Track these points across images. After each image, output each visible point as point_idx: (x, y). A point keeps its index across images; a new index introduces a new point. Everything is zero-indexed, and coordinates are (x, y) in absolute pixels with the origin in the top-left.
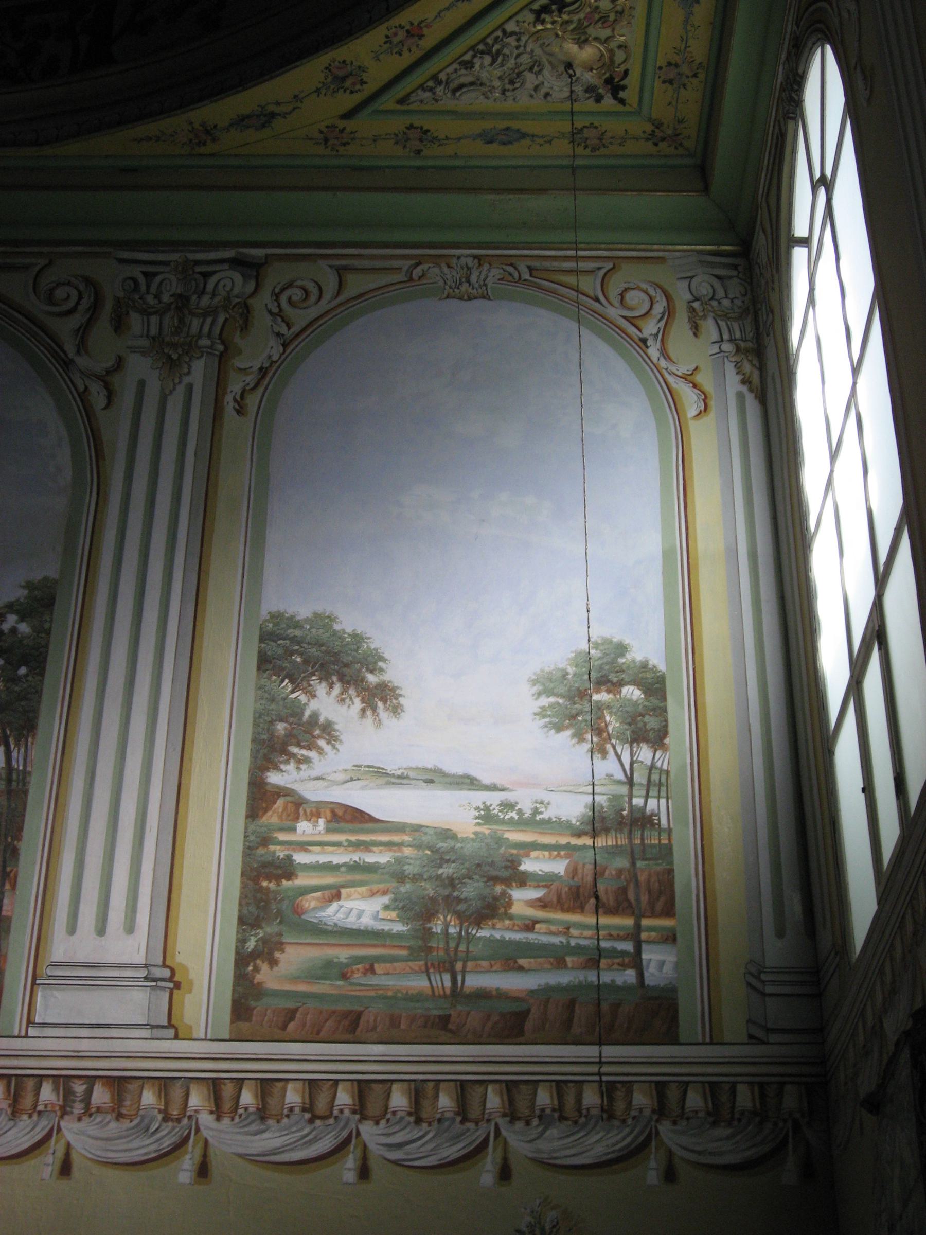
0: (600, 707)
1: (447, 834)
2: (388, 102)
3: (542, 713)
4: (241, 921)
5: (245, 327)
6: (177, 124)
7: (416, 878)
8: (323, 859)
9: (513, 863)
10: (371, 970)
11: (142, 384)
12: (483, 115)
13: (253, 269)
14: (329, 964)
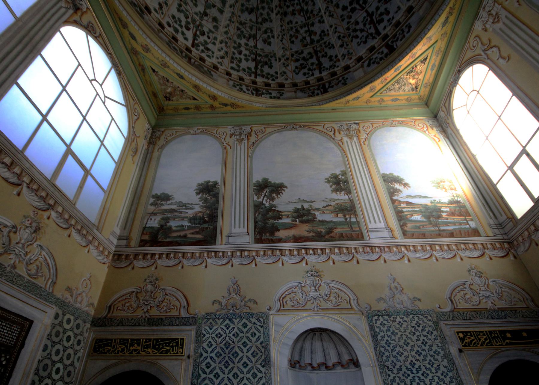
2: (378, 94)
6: (343, 100)
12: (393, 96)
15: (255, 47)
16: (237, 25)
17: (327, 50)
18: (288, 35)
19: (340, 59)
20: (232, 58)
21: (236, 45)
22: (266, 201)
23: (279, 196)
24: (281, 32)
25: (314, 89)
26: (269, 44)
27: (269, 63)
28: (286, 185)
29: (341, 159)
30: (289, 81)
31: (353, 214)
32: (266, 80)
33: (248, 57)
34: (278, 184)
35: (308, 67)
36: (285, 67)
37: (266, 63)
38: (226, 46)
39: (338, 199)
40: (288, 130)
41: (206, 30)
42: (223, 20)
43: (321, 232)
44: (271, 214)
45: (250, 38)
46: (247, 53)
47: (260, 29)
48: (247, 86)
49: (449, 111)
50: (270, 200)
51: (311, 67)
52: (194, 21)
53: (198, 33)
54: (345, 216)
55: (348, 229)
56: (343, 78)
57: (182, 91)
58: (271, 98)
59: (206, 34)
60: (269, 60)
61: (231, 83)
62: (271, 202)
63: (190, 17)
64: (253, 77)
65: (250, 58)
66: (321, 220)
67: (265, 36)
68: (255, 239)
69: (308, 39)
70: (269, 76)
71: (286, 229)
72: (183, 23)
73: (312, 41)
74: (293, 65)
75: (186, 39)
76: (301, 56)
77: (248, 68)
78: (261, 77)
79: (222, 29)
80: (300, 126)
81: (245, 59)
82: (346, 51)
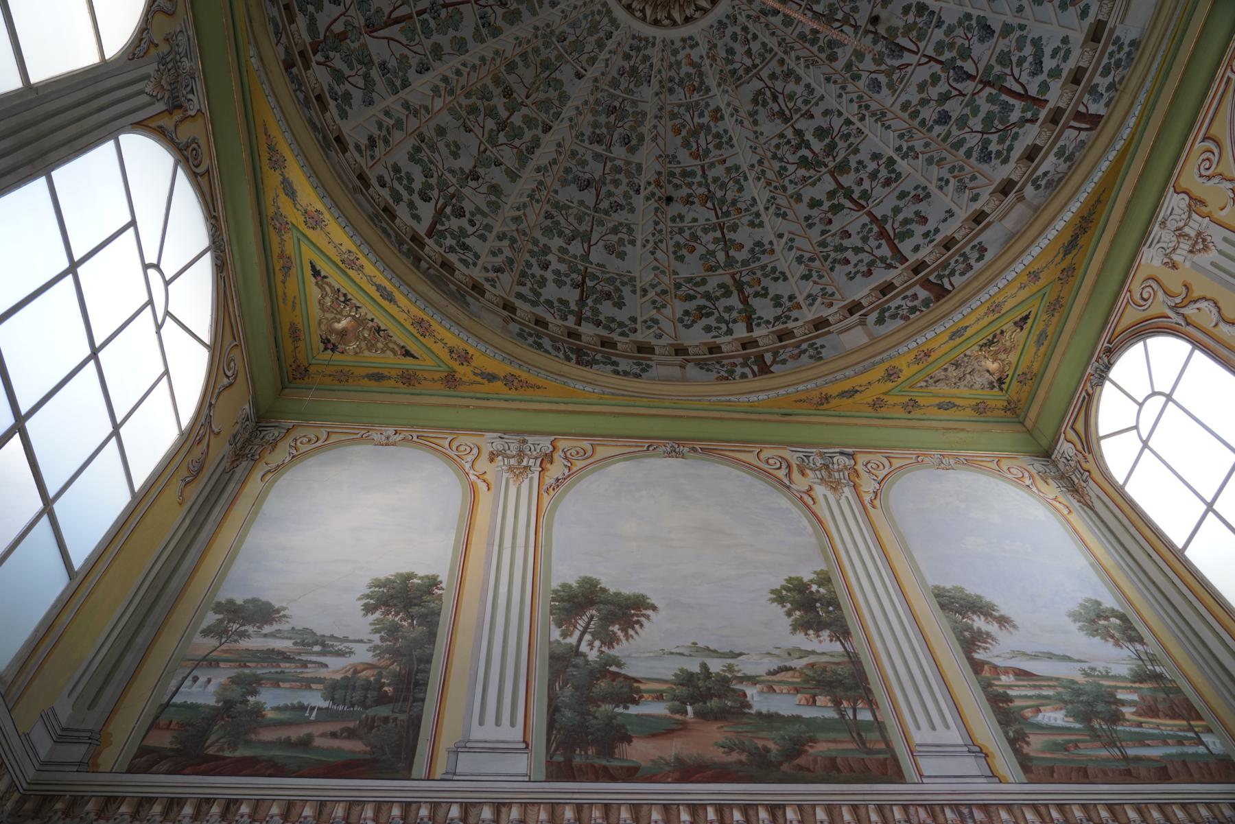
0: (1105, 627)
1: (1073, 682)
3: (1081, 629)
4: (1000, 723)
5: (858, 476)
7: (1072, 702)
8: (1023, 693)
9: (1113, 695)
10: (1077, 747)
11: (825, 496)
13: (851, 456)
14: (1055, 743)
15: (586, 257)
16: (547, 207)
17: (766, 282)
18: (671, 243)
20: (523, 274)
21: (536, 249)
22: (591, 644)
23: (631, 632)
24: (654, 235)
25: (735, 365)
26: (622, 256)
28: (653, 600)
29: (813, 540)
30: (665, 341)
31: (862, 697)
32: (605, 333)
33: (563, 278)
34: (628, 598)
35: (717, 314)
37: (608, 296)
38: (511, 247)
39: (813, 652)
40: (658, 456)
41: (468, 206)
42: (515, 194)
43: (767, 750)
44: (603, 684)
46: (563, 268)
47: (601, 223)
48: (554, 339)
49: (1088, 443)
50: (603, 643)
51: (726, 316)
52: (442, 186)
53: (448, 210)
54: (837, 704)
55: (852, 746)
56: (811, 345)
57: (379, 330)
58: (616, 372)
59: (467, 214)
60: (617, 289)
61: (514, 328)
62: (605, 649)
63: (435, 175)
64: (571, 322)
66: (764, 711)
67: (613, 238)
68: (549, 763)
69: (721, 256)
70: (612, 325)
71: (653, 736)
72: (417, 185)
74: (679, 307)
75: (417, 218)
76: (701, 289)
77: (560, 301)
78: (591, 325)
79: (507, 211)
80: (694, 450)
81: (556, 281)
82: (818, 287)
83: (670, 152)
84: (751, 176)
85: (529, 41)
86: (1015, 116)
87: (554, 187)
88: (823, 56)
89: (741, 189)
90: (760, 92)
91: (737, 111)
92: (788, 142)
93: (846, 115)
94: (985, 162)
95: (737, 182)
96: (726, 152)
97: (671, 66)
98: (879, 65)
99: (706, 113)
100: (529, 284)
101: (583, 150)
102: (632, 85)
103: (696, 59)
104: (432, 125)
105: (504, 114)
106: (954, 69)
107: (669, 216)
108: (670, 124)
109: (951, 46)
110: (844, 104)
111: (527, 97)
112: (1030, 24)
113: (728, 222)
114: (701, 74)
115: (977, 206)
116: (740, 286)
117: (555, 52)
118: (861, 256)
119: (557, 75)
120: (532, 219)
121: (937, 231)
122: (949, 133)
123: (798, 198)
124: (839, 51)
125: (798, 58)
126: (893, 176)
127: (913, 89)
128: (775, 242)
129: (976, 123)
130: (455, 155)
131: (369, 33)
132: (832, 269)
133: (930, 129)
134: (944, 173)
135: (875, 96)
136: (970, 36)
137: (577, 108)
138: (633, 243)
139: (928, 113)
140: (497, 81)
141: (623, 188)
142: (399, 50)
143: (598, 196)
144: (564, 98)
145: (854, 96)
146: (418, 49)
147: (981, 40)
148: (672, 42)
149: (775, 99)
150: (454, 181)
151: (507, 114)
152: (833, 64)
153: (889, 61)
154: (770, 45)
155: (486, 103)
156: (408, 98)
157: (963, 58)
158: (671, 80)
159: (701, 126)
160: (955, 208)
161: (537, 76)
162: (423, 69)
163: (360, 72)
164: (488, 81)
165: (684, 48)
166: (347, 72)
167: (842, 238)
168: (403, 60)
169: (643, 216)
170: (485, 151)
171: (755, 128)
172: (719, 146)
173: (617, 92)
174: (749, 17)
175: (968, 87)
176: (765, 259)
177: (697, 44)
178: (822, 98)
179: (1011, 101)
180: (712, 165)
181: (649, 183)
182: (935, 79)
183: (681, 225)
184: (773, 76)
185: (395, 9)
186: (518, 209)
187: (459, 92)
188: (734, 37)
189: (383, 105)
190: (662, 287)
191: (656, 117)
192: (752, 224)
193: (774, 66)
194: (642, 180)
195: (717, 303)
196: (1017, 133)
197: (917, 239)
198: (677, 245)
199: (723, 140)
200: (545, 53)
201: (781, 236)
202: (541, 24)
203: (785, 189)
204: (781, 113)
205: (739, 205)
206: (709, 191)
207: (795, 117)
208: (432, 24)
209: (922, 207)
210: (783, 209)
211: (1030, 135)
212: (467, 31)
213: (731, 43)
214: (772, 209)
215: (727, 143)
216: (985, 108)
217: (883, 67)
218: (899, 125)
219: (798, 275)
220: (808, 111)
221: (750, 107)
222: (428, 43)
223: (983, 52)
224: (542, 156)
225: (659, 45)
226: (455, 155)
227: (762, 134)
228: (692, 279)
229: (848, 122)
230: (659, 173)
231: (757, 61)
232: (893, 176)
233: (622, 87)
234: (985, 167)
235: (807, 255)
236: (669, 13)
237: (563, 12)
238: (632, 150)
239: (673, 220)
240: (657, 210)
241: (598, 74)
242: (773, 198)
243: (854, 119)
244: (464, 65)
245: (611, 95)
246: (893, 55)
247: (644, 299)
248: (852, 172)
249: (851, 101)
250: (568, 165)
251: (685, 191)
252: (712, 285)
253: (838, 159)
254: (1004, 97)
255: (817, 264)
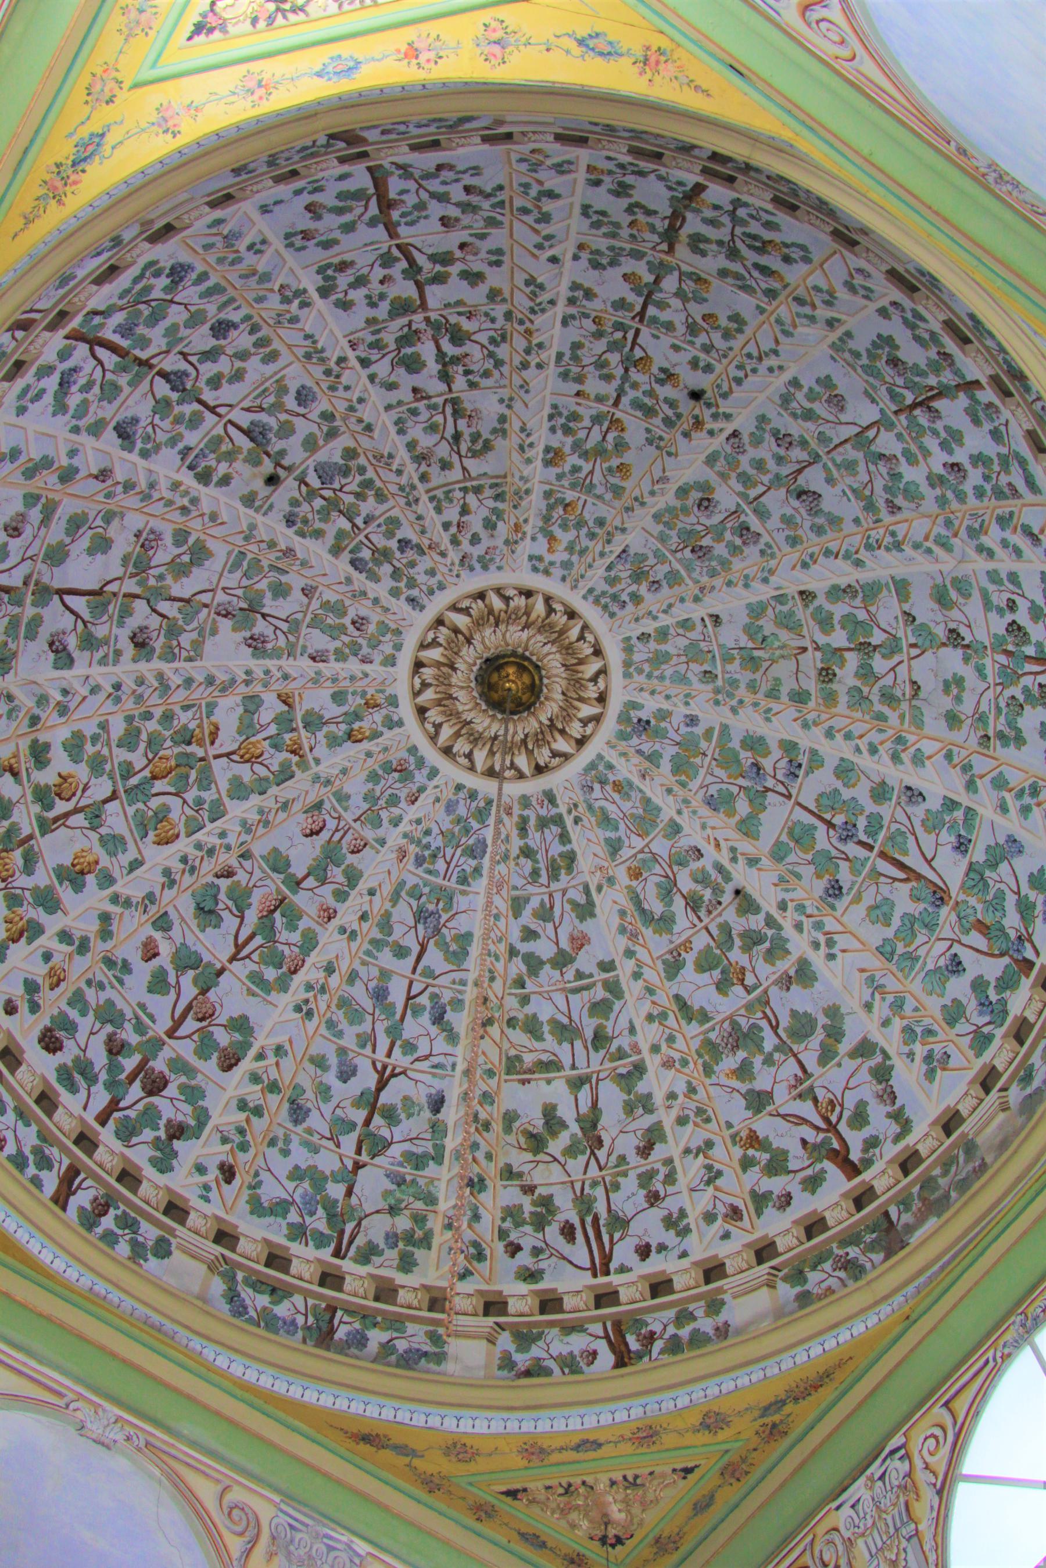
15: (882, 423)
18: (737, 343)
19: (583, 168)
20: (999, 493)
21: (949, 495)
24: (754, 371)
27: (884, 353)
33: (943, 435)
35: (738, 231)
36: (831, 293)
37: (894, 362)
38: (983, 530)
41: (999, 625)
45: (882, 456)
46: (932, 444)
47: (822, 438)
53: (1030, 651)
59: (1009, 617)
63: (1007, 693)
65: (939, 426)
67: (820, 409)
69: (670, 283)
70: (926, 336)
73: (660, 271)
74: (794, 274)
76: (736, 267)
77: (976, 422)
79: (947, 564)
82: (542, 175)
83: (651, 450)
84: (549, 355)
85: (755, 705)
86: (119, 318)
87: (854, 529)
88: (362, 461)
89: (576, 346)
90: (475, 454)
91: (521, 448)
92: (467, 373)
93: (364, 373)
94: (182, 266)
95: (575, 358)
96: (569, 404)
97: (583, 552)
98: (287, 422)
99: (567, 468)
100: (1004, 479)
101: (775, 534)
102: (652, 561)
103: (542, 541)
104: (958, 736)
105: (852, 660)
106: (184, 390)
107: (712, 377)
108: (627, 484)
109: (178, 420)
110: (360, 387)
111: (804, 650)
112: (64, 434)
113: (625, 317)
114: (547, 519)
115: (218, 214)
116: (670, 236)
117: (729, 667)
118: (442, 189)
119: (744, 641)
120: (919, 528)
121: (298, 193)
122: (220, 309)
123: (494, 295)
124: (337, 459)
125: (399, 472)
126: (330, 272)
127: (251, 377)
128: (569, 256)
129: (176, 315)
130: (959, 681)
131: (946, 891)
132: (500, 188)
133: (248, 318)
134: (250, 259)
135: (310, 383)
136: (150, 429)
137: (746, 586)
138: (795, 383)
139: (241, 339)
140: (830, 699)
141: (752, 453)
142: (927, 841)
143: (799, 471)
144: (756, 611)
145: (341, 393)
146: (901, 817)
147: (135, 421)
148: (564, 579)
149: (457, 437)
150: (988, 661)
151: (847, 655)
152: (352, 444)
153: (272, 422)
154: (431, 506)
155: (865, 690)
156: (962, 790)
157: (167, 403)
158: (592, 536)
159: (585, 455)
160: (255, 215)
161: (773, 661)
162: (913, 795)
163: (994, 875)
164: (842, 707)
165: (551, 564)
166: (1011, 900)
167: (457, 220)
168: (933, 823)
169: (751, 403)
170: (913, 646)
171: (507, 412)
172: (574, 417)
173: (677, 566)
174: (443, 554)
175: (172, 363)
176: (602, 244)
177: (531, 558)
178: (388, 408)
179: (116, 339)
180: (600, 399)
181: (711, 433)
182: (215, 383)
183: (702, 356)
184: (445, 465)
185: (895, 879)
186: (929, 551)
187: (891, 732)
188: (475, 540)
189: (998, 819)
190: (796, 308)
191: (643, 504)
192: (589, 294)
193: (438, 477)
194: (718, 443)
195: (727, 238)
196: (121, 298)
197: (334, 189)
198: (727, 335)
199: (564, 421)
200: (744, 677)
201: (554, 260)
202: (726, 710)
203: (508, 316)
204: (457, 413)
205: (593, 328)
206: (626, 370)
207: (440, 401)
208: (862, 823)
209: (305, 222)
210: (528, 290)
211: (101, 297)
212: (822, 780)
213: (483, 534)
214: (544, 297)
215: (560, 414)
216: (157, 336)
217: (283, 417)
218: (290, 335)
219: (560, 203)
220: (417, 400)
221: (499, 443)
222: (886, 810)
223: (137, 403)
224: (844, 574)
225: (584, 587)
226: (959, 681)
227: (501, 401)
228: (740, 288)
229: (365, 363)
230: (686, 435)
231: (459, 494)
232: (330, 272)
233: (666, 568)
234: (185, 257)
235: (529, 219)
236: (548, 615)
237: (687, 704)
238: (705, 487)
239: (708, 369)
240: (725, 396)
241: (689, 605)
242: (533, 311)
243: (353, 362)
244: (858, 750)
245: (689, 569)
246: (264, 430)
247: (843, 317)
248: (391, 296)
249: (347, 388)
250: (812, 536)
251: (665, 391)
252: (711, 263)
253: (404, 320)
254: (125, 343)
255: (518, 203)
